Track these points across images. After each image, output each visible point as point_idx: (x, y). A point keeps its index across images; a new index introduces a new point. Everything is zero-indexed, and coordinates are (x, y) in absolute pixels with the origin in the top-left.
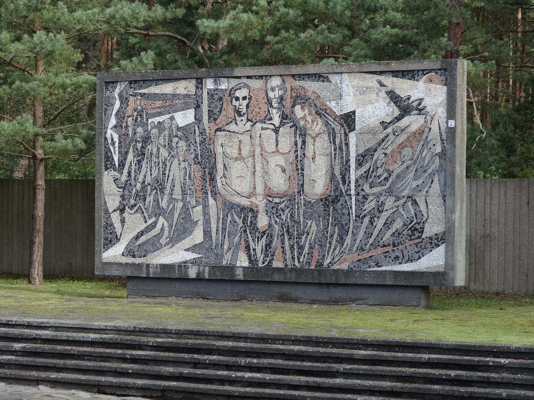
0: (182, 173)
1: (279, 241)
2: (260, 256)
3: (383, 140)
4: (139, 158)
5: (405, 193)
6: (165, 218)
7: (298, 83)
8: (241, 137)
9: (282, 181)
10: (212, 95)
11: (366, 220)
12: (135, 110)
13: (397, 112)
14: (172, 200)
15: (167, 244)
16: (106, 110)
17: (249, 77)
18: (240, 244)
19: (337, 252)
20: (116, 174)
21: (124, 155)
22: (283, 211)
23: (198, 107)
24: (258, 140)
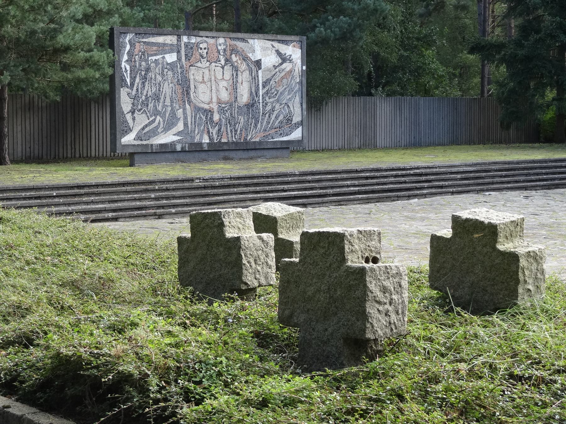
0: (171, 90)
1: (225, 128)
2: (215, 136)
3: (274, 75)
4: (143, 81)
6: (161, 117)
7: (233, 42)
8: (204, 71)
9: (226, 95)
10: (187, 46)
11: (267, 115)
12: (140, 51)
13: (280, 61)
14: (164, 106)
15: (162, 132)
16: (121, 50)
17: (207, 37)
18: (204, 130)
19: (253, 132)
20: (129, 90)
21: (133, 79)
22: (227, 111)
23: (179, 52)
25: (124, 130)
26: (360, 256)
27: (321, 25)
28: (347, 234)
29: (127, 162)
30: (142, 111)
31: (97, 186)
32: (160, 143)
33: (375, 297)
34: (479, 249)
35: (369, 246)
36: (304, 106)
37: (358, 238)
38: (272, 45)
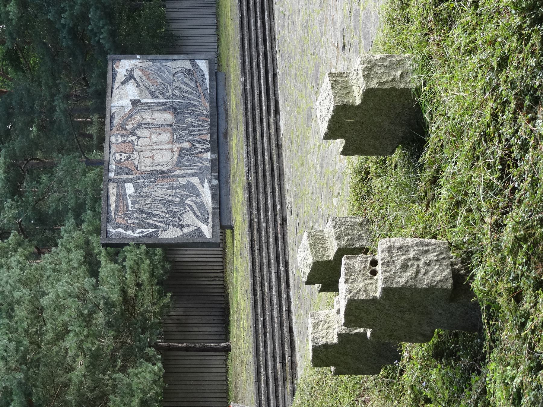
0: (161, 189)
2: (205, 146)
5: (172, 77)
6: (186, 199)
8: (142, 156)
9: (165, 135)
10: (118, 173)
11: (184, 94)
13: (132, 81)
14: (176, 196)
15: (200, 198)
17: (110, 153)
19: (201, 108)
21: (150, 226)
23: (124, 181)
24: (143, 148)
25: (199, 235)
26: (370, 281)
27: (96, 36)
28: (348, 297)
29: (228, 232)
30: (181, 218)
31: (254, 277)
32: (211, 200)
33: (411, 279)
34: (358, 119)
35: (360, 271)
36: (176, 57)
37: (352, 283)
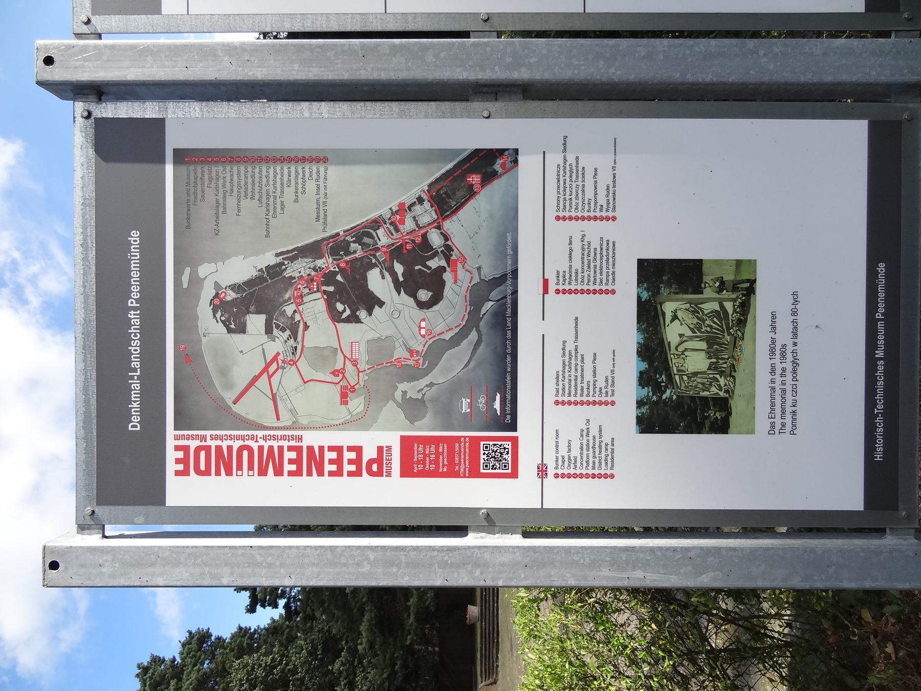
11: (713, 330)
38: (668, 326)
